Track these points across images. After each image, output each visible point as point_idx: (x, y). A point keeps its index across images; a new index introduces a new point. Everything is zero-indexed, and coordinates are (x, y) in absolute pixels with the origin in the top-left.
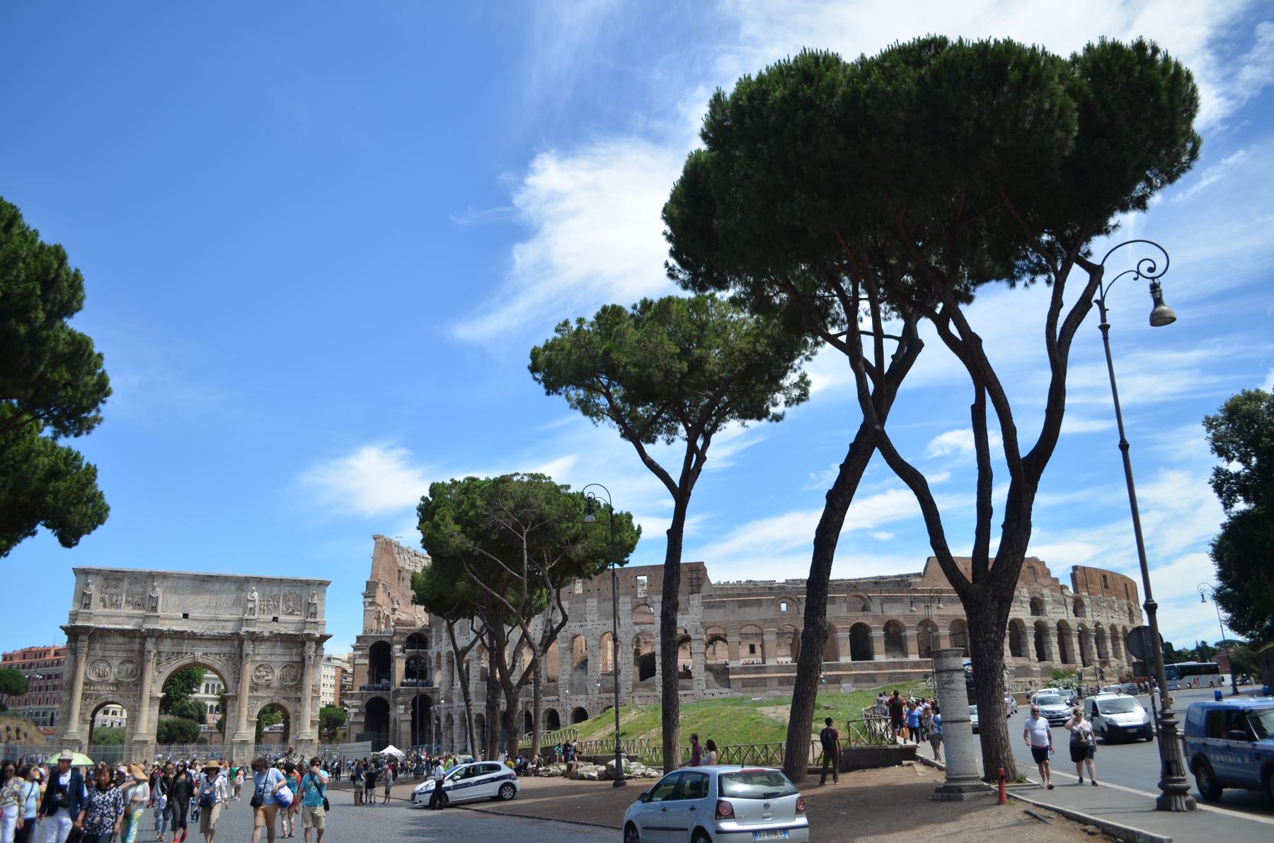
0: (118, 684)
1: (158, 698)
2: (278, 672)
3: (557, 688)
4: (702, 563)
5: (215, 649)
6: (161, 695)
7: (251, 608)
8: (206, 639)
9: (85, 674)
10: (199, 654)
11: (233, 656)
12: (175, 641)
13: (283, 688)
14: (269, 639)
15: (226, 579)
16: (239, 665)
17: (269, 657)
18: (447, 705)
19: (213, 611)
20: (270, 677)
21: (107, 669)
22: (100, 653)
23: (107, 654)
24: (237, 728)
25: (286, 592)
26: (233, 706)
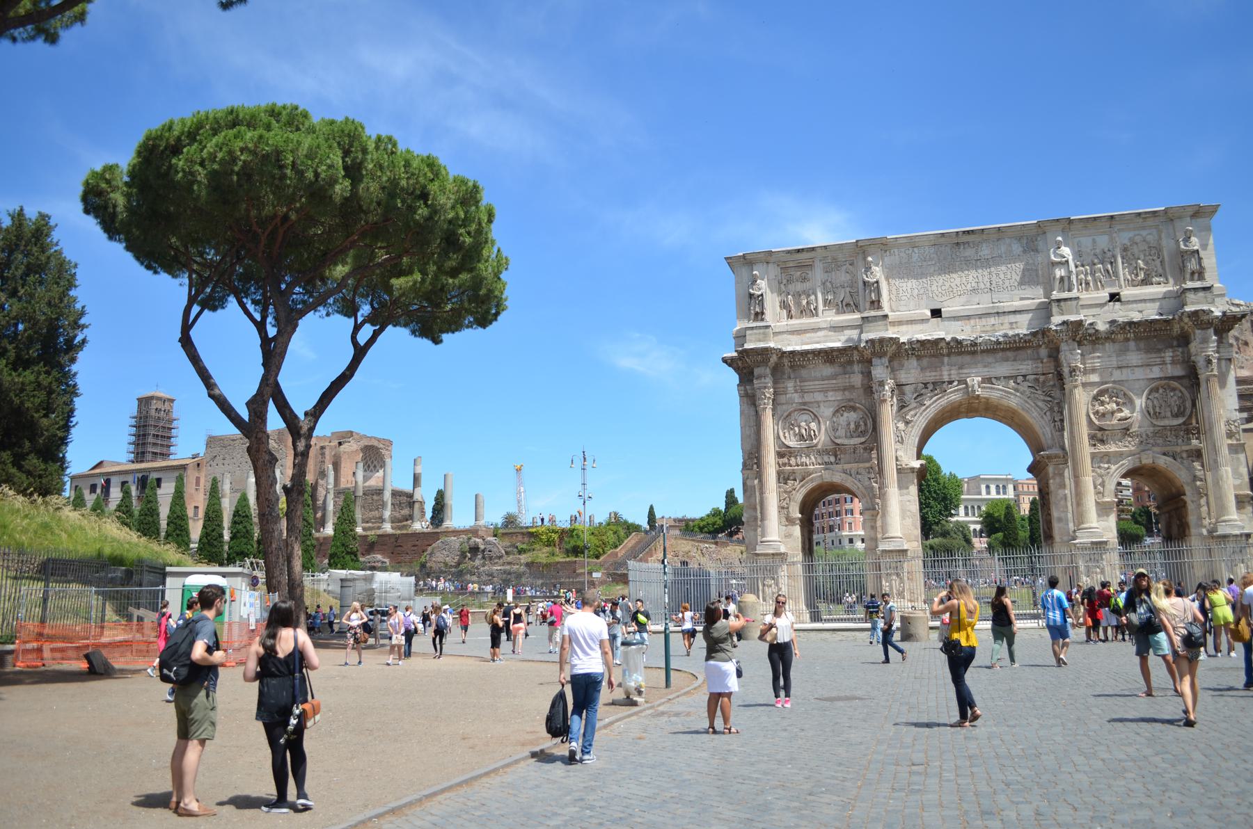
0: (835, 451)
2: (1140, 402)
5: (1003, 369)
6: (917, 464)
7: (1062, 279)
8: (983, 351)
10: (975, 381)
12: (925, 361)
14: (1109, 337)
16: (1056, 393)
19: (987, 297)
21: (813, 425)
22: (797, 398)
23: (808, 398)
24: (1080, 518)
25: (1127, 242)
26: (1062, 475)
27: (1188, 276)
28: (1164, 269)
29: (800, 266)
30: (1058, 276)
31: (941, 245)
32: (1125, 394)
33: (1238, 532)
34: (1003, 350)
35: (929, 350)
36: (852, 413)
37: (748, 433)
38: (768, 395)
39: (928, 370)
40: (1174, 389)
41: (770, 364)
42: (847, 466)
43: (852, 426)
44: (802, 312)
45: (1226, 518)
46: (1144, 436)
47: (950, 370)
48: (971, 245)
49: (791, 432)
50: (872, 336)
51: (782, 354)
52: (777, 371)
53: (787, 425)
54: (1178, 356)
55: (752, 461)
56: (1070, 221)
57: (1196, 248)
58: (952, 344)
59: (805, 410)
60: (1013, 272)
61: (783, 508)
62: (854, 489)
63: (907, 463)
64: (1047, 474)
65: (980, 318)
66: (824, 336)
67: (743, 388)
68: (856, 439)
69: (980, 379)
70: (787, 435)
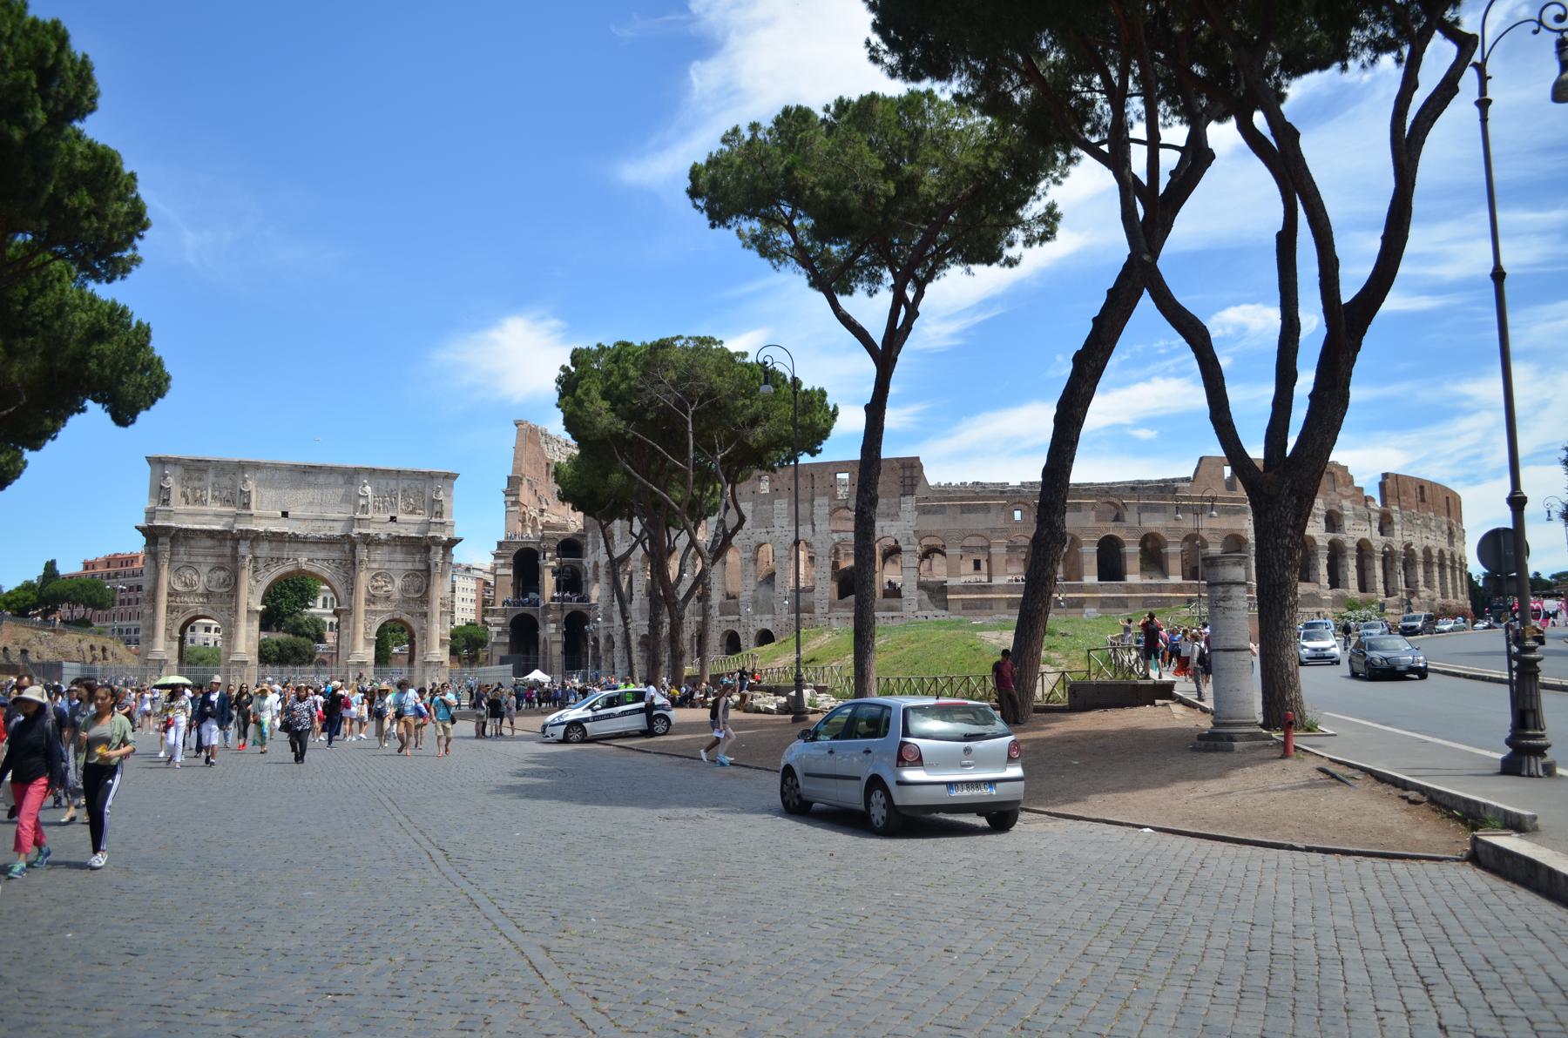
0: (208, 595)
1: (257, 611)
2: (398, 582)
3: (738, 605)
4: (918, 458)
5: (321, 555)
6: (260, 608)
7: (363, 506)
9: (169, 583)
10: (303, 560)
11: (344, 563)
12: (274, 544)
13: (406, 601)
14: (386, 543)
15: (332, 470)
16: (351, 573)
18: (606, 624)
19: (317, 509)
20: (389, 588)
21: (195, 577)
22: (185, 558)
23: (193, 559)
24: (353, 647)
25: (406, 487)
26: (347, 621)
35: (278, 538)
40: (418, 577)
43: (221, 580)
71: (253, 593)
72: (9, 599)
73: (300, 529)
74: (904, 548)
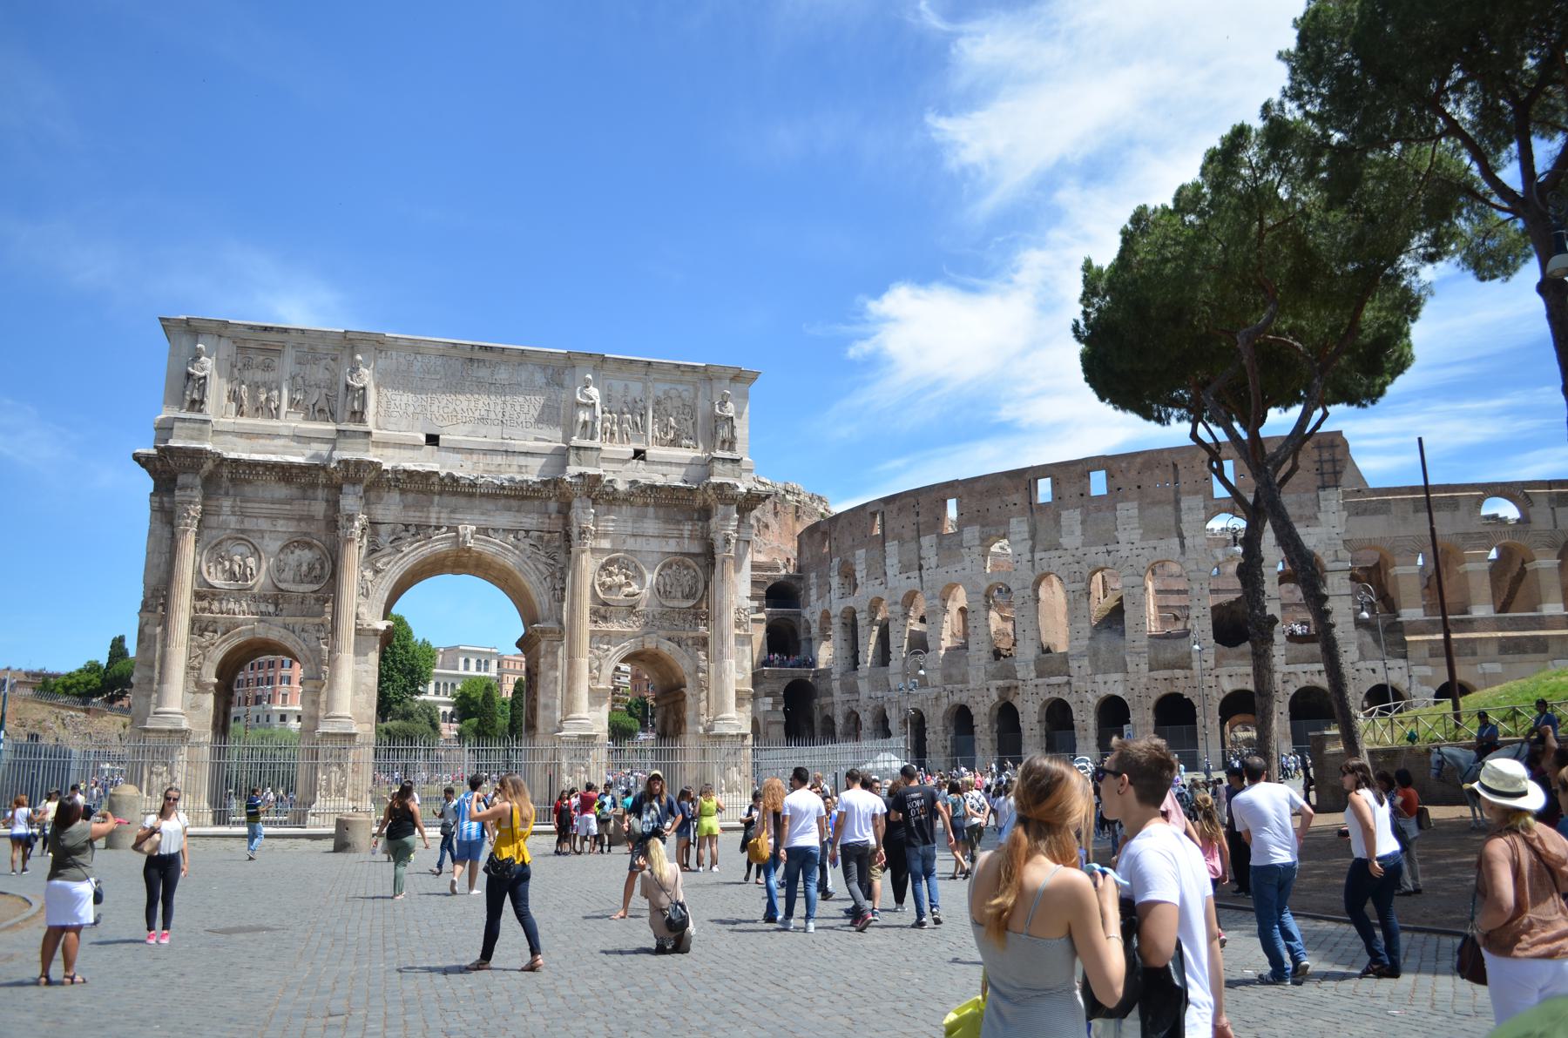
0: (277, 598)
2: (651, 578)
4: (1339, 433)
5: (503, 520)
6: (382, 625)
7: (585, 423)
8: (482, 495)
10: (467, 529)
12: (410, 497)
14: (627, 499)
16: (561, 556)
17: (630, 541)
20: (634, 588)
21: (251, 561)
22: (233, 522)
24: (569, 706)
25: (660, 394)
26: (555, 654)
27: (719, 444)
28: (695, 432)
29: (265, 349)
30: (581, 420)
31: (451, 357)
32: (636, 567)
33: (735, 733)
34: (507, 497)
35: (418, 484)
36: (306, 551)
37: (156, 561)
38: (192, 513)
39: (413, 509)
40: (688, 567)
41: (201, 471)
42: (290, 620)
43: (304, 568)
44: (257, 409)
45: (721, 716)
46: (651, 617)
47: (440, 512)
48: (487, 364)
49: (219, 567)
50: (347, 455)
51: (221, 461)
52: (211, 485)
53: (215, 556)
54: (696, 530)
55: (157, 601)
56: (604, 359)
57: (730, 415)
58: (446, 480)
59: (242, 539)
60: (531, 406)
61: (193, 668)
62: (296, 651)
63: (370, 622)
64: (538, 651)
65: (485, 454)
66: (284, 446)
67: (157, 499)
68: (306, 586)
69: (474, 528)
70: (212, 570)
71: (367, 596)
72: (69, 682)
73: (463, 469)
74: (1329, 566)
